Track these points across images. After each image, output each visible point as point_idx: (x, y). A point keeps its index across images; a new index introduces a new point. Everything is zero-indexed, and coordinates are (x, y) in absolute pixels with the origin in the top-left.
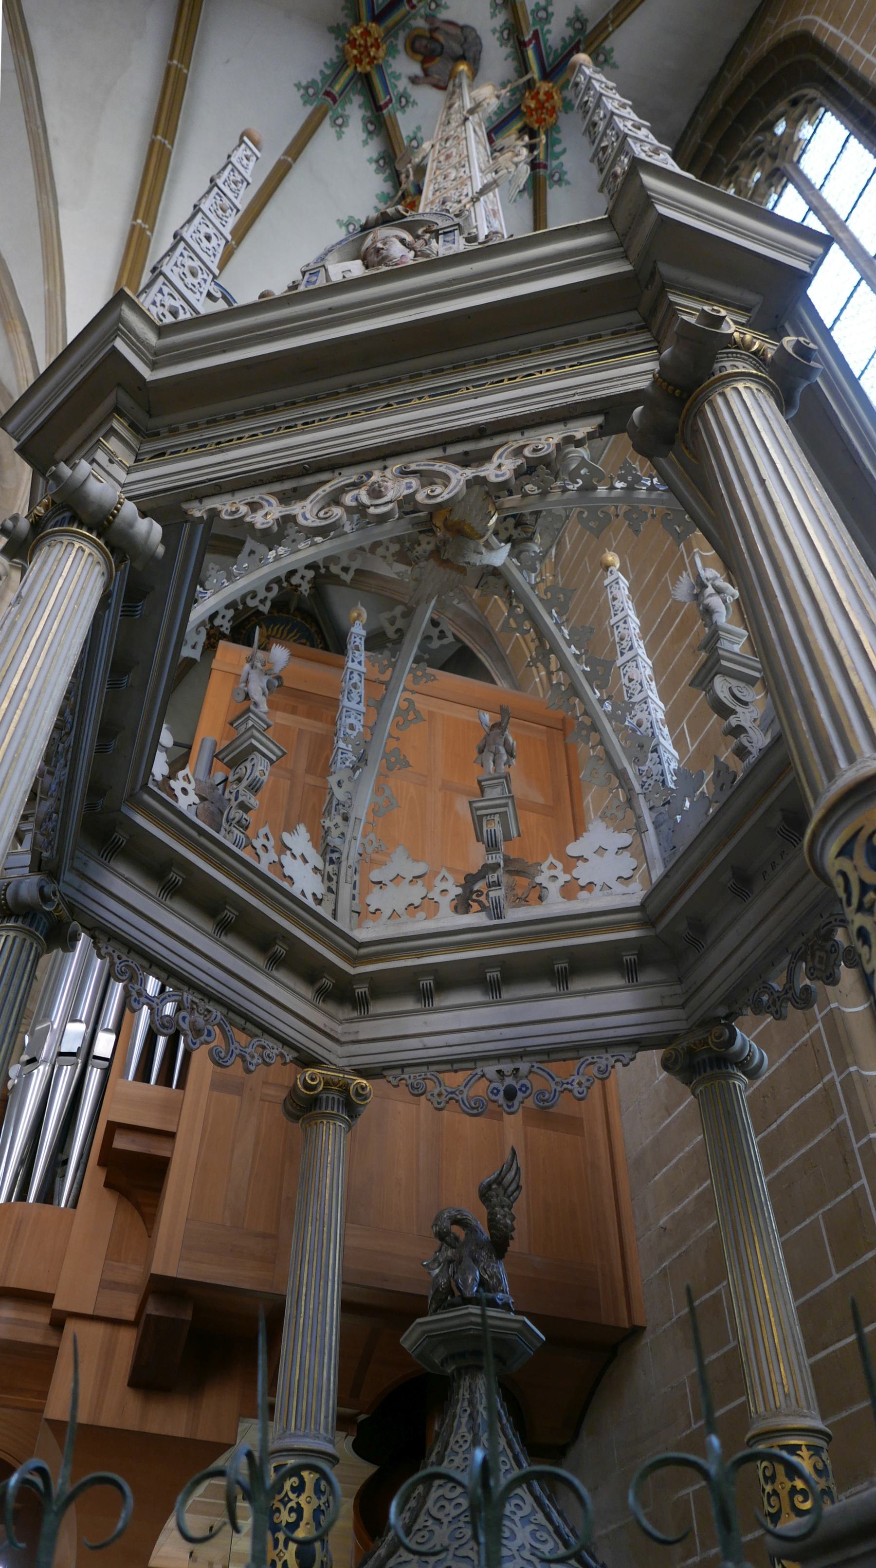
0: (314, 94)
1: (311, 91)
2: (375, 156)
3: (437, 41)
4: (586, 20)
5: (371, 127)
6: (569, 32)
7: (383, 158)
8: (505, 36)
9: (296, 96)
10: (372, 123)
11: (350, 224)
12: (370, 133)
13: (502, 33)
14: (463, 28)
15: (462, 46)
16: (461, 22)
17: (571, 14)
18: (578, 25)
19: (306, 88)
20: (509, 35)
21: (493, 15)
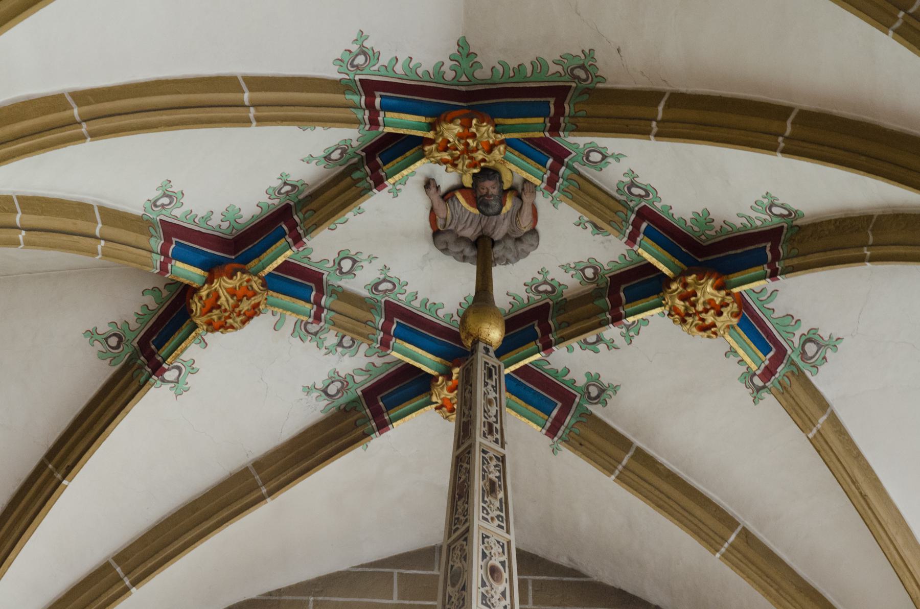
0: (357, 67)
1: (360, 60)
2: (294, 178)
3: (502, 204)
4: (605, 403)
5: (336, 155)
6: (581, 381)
7: (294, 187)
8: (542, 288)
9: (345, 42)
10: (344, 152)
11: (170, 197)
12: (327, 158)
13: (545, 282)
14: (534, 232)
15: (507, 236)
16: (539, 227)
17: (605, 380)
18: (594, 391)
19: (363, 52)
20: (546, 292)
21: (566, 268)
